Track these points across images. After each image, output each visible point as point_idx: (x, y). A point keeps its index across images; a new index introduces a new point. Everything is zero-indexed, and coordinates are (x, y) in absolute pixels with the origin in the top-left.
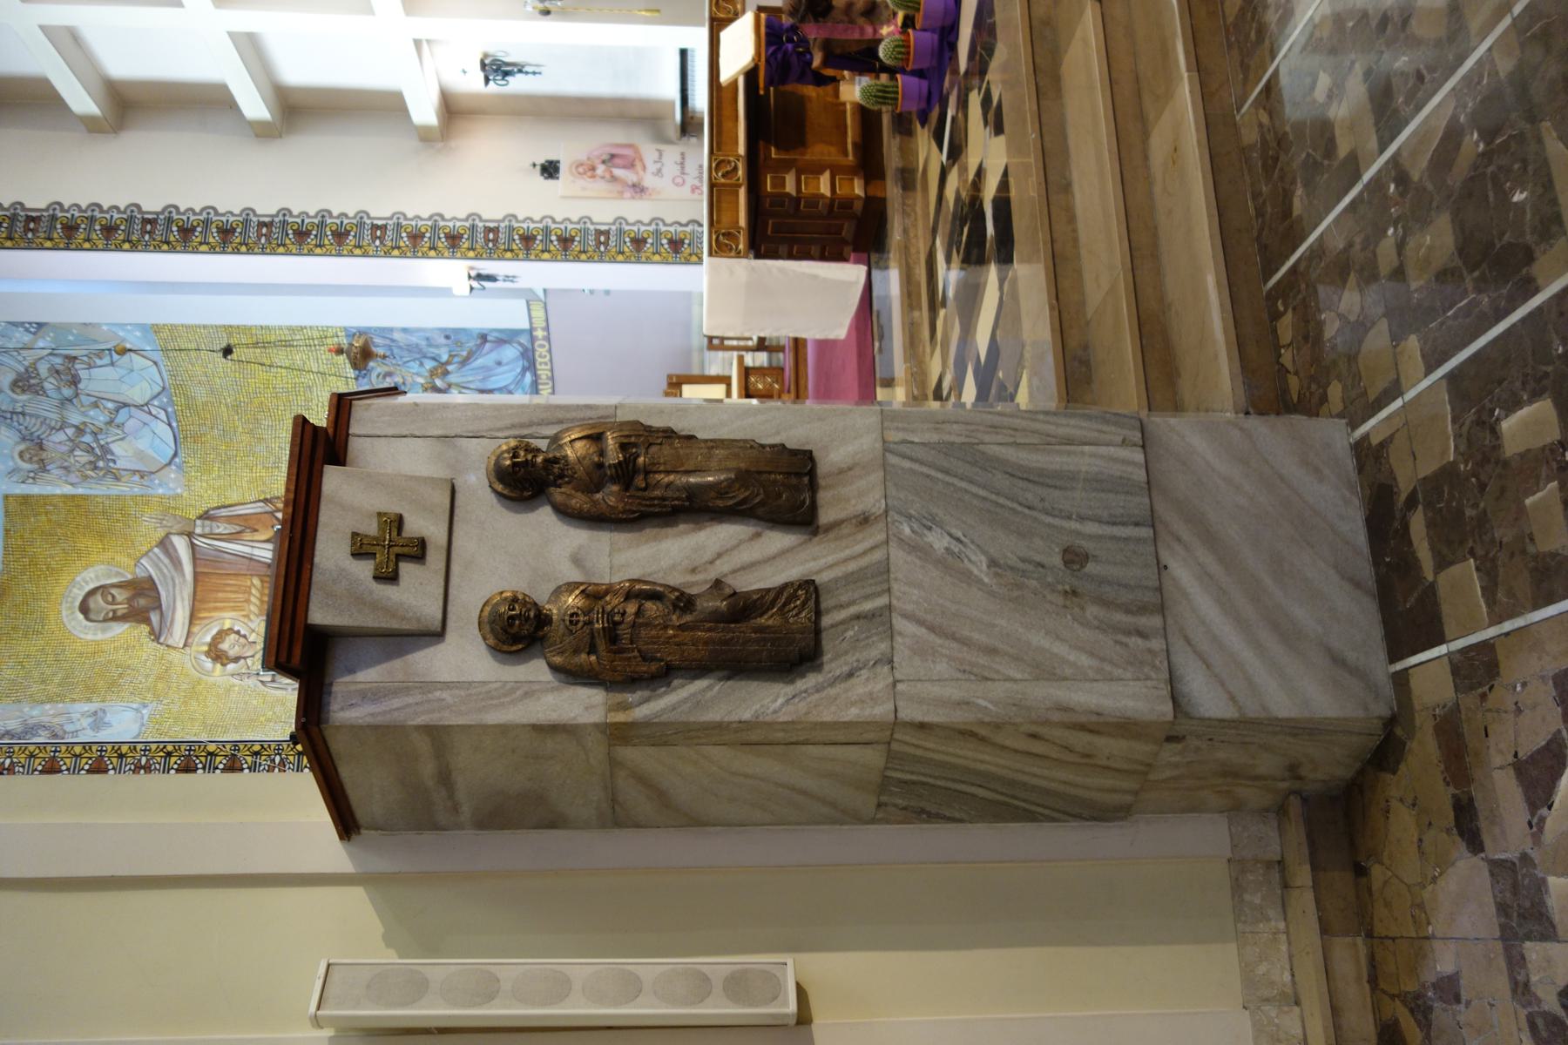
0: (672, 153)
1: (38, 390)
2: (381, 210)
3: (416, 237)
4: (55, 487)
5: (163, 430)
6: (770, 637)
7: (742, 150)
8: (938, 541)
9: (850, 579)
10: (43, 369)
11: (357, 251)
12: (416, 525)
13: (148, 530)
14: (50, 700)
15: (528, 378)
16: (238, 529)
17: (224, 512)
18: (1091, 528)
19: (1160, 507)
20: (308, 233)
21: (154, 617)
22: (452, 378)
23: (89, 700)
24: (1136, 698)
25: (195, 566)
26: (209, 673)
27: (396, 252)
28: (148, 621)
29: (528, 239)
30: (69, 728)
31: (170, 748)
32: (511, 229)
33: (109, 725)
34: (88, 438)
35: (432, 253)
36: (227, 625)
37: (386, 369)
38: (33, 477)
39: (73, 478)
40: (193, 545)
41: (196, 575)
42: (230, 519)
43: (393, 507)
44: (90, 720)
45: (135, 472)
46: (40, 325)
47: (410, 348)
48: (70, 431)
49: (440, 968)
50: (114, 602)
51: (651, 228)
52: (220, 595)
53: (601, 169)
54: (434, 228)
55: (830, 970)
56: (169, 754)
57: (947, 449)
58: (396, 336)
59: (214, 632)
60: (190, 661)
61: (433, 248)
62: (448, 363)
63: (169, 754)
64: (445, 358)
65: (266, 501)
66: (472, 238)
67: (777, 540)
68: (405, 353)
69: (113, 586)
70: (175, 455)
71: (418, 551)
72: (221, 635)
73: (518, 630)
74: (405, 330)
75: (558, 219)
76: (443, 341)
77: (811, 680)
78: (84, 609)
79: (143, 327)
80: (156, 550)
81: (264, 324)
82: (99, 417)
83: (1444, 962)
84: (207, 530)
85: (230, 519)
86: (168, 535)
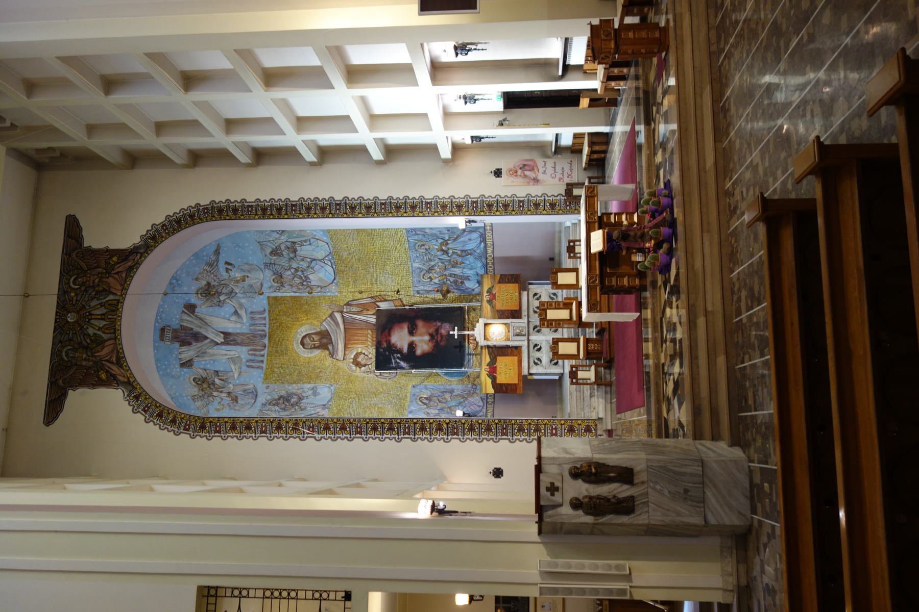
0: (550, 163)
1: (281, 255)
2: (429, 195)
3: (444, 207)
4: (287, 293)
5: (329, 269)
6: (625, 506)
7: (598, 272)
8: (658, 487)
9: (640, 495)
10: (283, 247)
12: (557, 484)
13: (325, 311)
14: (295, 383)
15: (483, 245)
17: (355, 302)
18: (690, 485)
19: (705, 480)
20: (400, 207)
21: (330, 347)
22: (449, 246)
23: (310, 383)
24: (697, 520)
26: (355, 372)
28: (328, 349)
29: (490, 206)
30: (304, 395)
32: (483, 201)
33: (319, 394)
34: (300, 273)
38: (278, 289)
39: (294, 289)
41: (345, 329)
42: (358, 305)
43: (552, 481)
46: (283, 231)
47: (432, 235)
48: (293, 271)
49: (561, 561)
53: (519, 172)
54: (451, 202)
55: (636, 564)
57: (661, 467)
60: (347, 366)
61: (451, 211)
65: (372, 297)
66: (467, 207)
67: (626, 487)
71: (557, 489)
72: (357, 355)
73: (576, 504)
74: (431, 229)
77: (633, 515)
78: (302, 343)
79: (323, 231)
82: (304, 265)
83: (755, 574)
85: (358, 305)
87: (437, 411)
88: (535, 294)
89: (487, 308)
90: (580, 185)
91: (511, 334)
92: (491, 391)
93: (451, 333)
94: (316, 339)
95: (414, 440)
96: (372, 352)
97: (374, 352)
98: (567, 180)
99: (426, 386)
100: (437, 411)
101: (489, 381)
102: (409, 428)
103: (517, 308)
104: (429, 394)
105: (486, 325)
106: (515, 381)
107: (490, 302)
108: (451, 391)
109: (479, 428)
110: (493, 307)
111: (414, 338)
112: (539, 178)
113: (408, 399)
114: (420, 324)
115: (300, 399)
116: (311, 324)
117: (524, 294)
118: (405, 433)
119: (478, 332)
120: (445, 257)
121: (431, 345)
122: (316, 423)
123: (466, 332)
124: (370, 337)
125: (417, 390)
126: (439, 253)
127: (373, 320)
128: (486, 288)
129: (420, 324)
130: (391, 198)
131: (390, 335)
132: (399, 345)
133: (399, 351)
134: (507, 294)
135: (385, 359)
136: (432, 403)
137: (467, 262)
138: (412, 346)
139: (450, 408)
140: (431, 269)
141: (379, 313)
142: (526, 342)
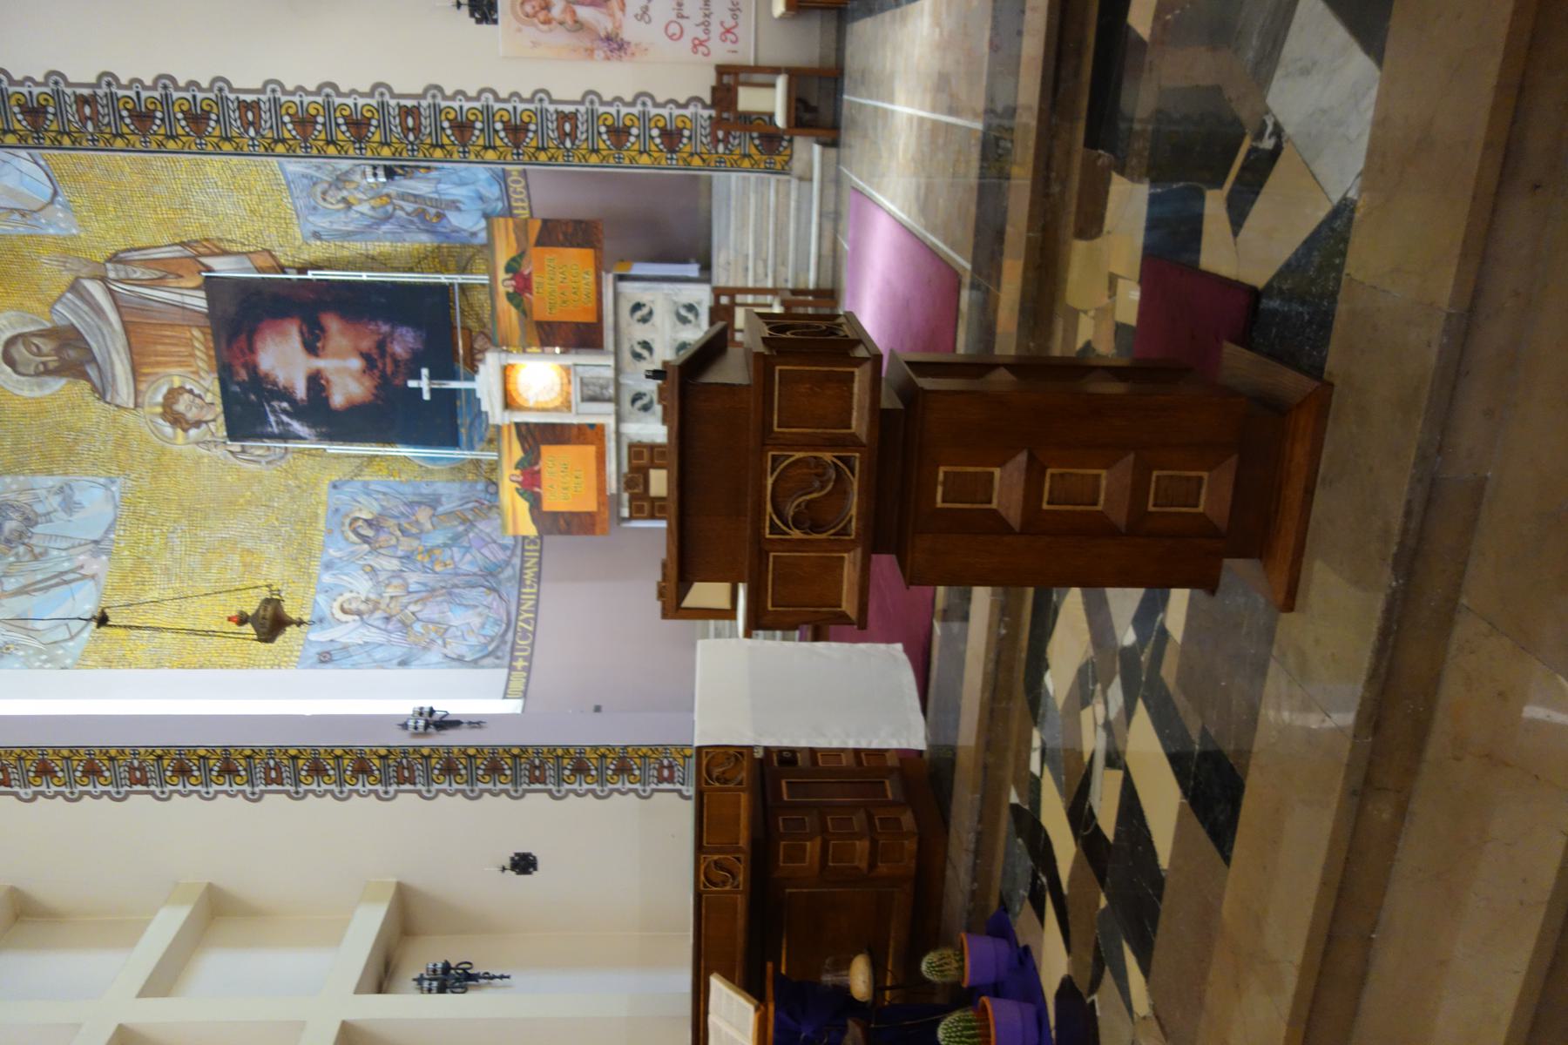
2: (246, 78)
11: (227, 147)
14: (8, 472)
16: (159, 274)
17: (136, 256)
23: (50, 473)
25: (120, 315)
26: (171, 441)
27: (280, 148)
30: (39, 508)
31: (159, 752)
36: (177, 384)
41: (124, 324)
42: (147, 263)
44: (58, 499)
45: (12, 210)
50: (39, 353)
51: (636, 110)
52: (160, 348)
54: (328, 107)
56: (160, 758)
59: (164, 390)
60: (147, 424)
61: (331, 142)
63: (160, 758)
65: (182, 244)
69: (33, 334)
70: (55, 193)
72: (173, 395)
75: (503, 94)
78: (10, 362)
80: (69, 295)
84: (122, 275)
85: (147, 263)
86: (77, 279)
87: (394, 564)
88: (637, 307)
89: (509, 315)
90: (760, 74)
91: (575, 397)
92: (529, 529)
93: (412, 384)
95: (296, 796)
96: (209, 387)
97: (216, 387)
98: (722, 53)
99: (366, 484)
100: (394, 564)
101: (523, 506)
102: (277, 768)
103: (591, 318)
104: (376, 508)
105: (506, 371)
106: (590, 505)
107: (516, 298)
108: (433, 502)
109: (471, 768)
110: (524, 312)
111: (320, 363)
112: (626, 35)
113: (322, 525)
114: (333, 324)
115: (30, 521)
116: (20, 308)
117: (608, 280)
118: (269, 781)
119: (485, 384)
121: (368, 383)
122: (12, 760)
123: (454, 385)
124: (199, 343)
125: (343, 497)
127: (199, 301)
128: (502, 259)
129: (333, 324)
130: (108, 78)
131: (252, 349)
132: (282, 378)
133: (286, 394)
134: (565, 278)
135: (249, 410)
136: (383, 537)
138: (316, 382)
141: (213, 286)
142: (610, 422)
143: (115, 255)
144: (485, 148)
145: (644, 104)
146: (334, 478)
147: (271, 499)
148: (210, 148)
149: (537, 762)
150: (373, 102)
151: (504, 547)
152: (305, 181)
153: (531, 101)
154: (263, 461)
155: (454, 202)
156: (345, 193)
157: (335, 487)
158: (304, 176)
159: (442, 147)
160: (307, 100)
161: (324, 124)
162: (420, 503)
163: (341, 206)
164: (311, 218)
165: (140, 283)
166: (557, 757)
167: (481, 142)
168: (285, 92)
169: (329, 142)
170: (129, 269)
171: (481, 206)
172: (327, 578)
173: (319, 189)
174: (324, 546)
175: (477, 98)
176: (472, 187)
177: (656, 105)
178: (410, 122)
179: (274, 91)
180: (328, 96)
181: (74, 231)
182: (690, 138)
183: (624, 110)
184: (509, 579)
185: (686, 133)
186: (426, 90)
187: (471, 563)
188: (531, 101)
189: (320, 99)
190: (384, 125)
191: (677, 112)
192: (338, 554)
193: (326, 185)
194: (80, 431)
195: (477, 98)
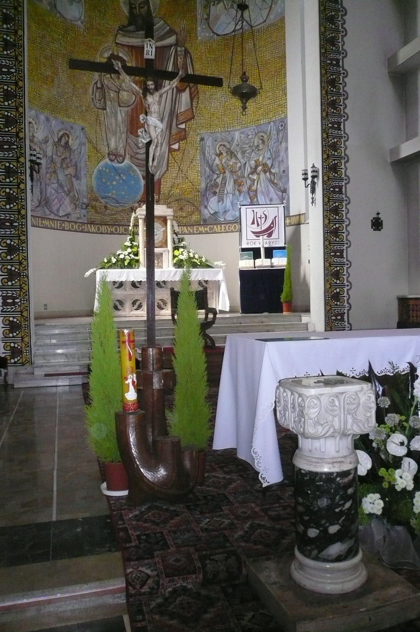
2: (349, 127)
5: (231, 28)
17: (189, 61)
21: (131, 28)
22: (262, 176)
28: (130, 24)
32: (342, 201)
35: (325, 156)
37: (266, 140)
40: (171, 46)
47: (277, 152)
50: (140, 8)
54: (340, 157)
58: (283, 144)
59: (125, 58)
62: (270, 173)
64: (273, 171)
68: (275, 149)
70: (218, 35)
74: (287, 149)
75: (349, 228)
76: (282, 170)
79: (283, 12)
80: (168, 28)
81: (287, 74)
84: (179, 53)
94: (142, 10)
100: (49, 153)
104: (74, 148)
108: (77, 177)
120: (248, 170)
125: (78, 132)
126: (253, 163)
136: (61, 149)
137: (241, 198)
139: (55, 172)
140: (232, 154)
143: (189, 52)
144: (329, 219)
145: (348, 286)
146: (86, 129)
147: (76, 97)
148: (324, 107)
149: (16, 224)
150: (343, 176)
151: (58, 210)
152: (230, 139)
153: (347, 240)
154: (93, 97)
155: (223, 200)
156: (225, 154)
157: (83, 129)
158: (233, 139)
159: (329, 202)
160: (343, 149)
161: (334, 155)
162: (76, 169)
163: (218, 152)
164: (211, 138)
165: (175, 60)
166: (19, 236)
167: (331, 218)
168: (345, 141)
169: (328, 155)
170: (182, 57)
171: (221, 211)
172: (42, 117)
173: (226, 144)
174: (55, 118)
175: (347, 218)
176: (231, 208)
177: (348, 290)
178: (337, 190)
179: (345, 137)
180: (344, 158)
181: (199, 38)
182: (336, 305)
183: (345, 277)
184: (44, 212)
185: (338, 303)
186: (348, 197)
187: (51, 192)
188: (347, 240)
189: (343, 154)
190: (335, 179)
191: (345, 298)
192: (53, 125)
193: (228, 147)
194: (104, 15)
195: (347, 218)
